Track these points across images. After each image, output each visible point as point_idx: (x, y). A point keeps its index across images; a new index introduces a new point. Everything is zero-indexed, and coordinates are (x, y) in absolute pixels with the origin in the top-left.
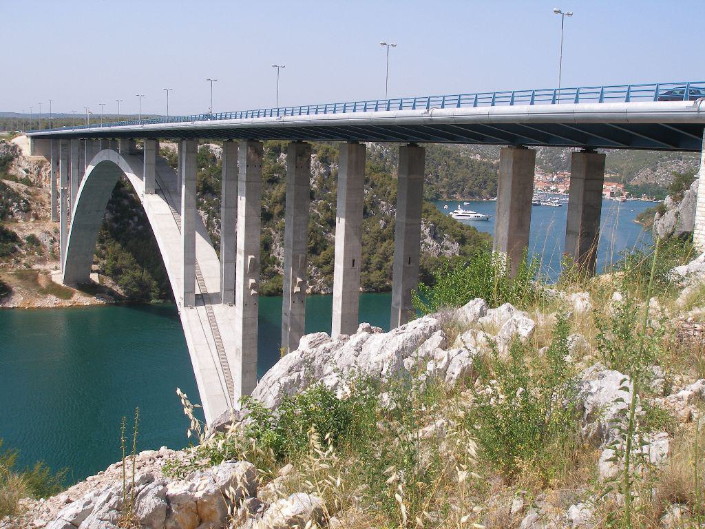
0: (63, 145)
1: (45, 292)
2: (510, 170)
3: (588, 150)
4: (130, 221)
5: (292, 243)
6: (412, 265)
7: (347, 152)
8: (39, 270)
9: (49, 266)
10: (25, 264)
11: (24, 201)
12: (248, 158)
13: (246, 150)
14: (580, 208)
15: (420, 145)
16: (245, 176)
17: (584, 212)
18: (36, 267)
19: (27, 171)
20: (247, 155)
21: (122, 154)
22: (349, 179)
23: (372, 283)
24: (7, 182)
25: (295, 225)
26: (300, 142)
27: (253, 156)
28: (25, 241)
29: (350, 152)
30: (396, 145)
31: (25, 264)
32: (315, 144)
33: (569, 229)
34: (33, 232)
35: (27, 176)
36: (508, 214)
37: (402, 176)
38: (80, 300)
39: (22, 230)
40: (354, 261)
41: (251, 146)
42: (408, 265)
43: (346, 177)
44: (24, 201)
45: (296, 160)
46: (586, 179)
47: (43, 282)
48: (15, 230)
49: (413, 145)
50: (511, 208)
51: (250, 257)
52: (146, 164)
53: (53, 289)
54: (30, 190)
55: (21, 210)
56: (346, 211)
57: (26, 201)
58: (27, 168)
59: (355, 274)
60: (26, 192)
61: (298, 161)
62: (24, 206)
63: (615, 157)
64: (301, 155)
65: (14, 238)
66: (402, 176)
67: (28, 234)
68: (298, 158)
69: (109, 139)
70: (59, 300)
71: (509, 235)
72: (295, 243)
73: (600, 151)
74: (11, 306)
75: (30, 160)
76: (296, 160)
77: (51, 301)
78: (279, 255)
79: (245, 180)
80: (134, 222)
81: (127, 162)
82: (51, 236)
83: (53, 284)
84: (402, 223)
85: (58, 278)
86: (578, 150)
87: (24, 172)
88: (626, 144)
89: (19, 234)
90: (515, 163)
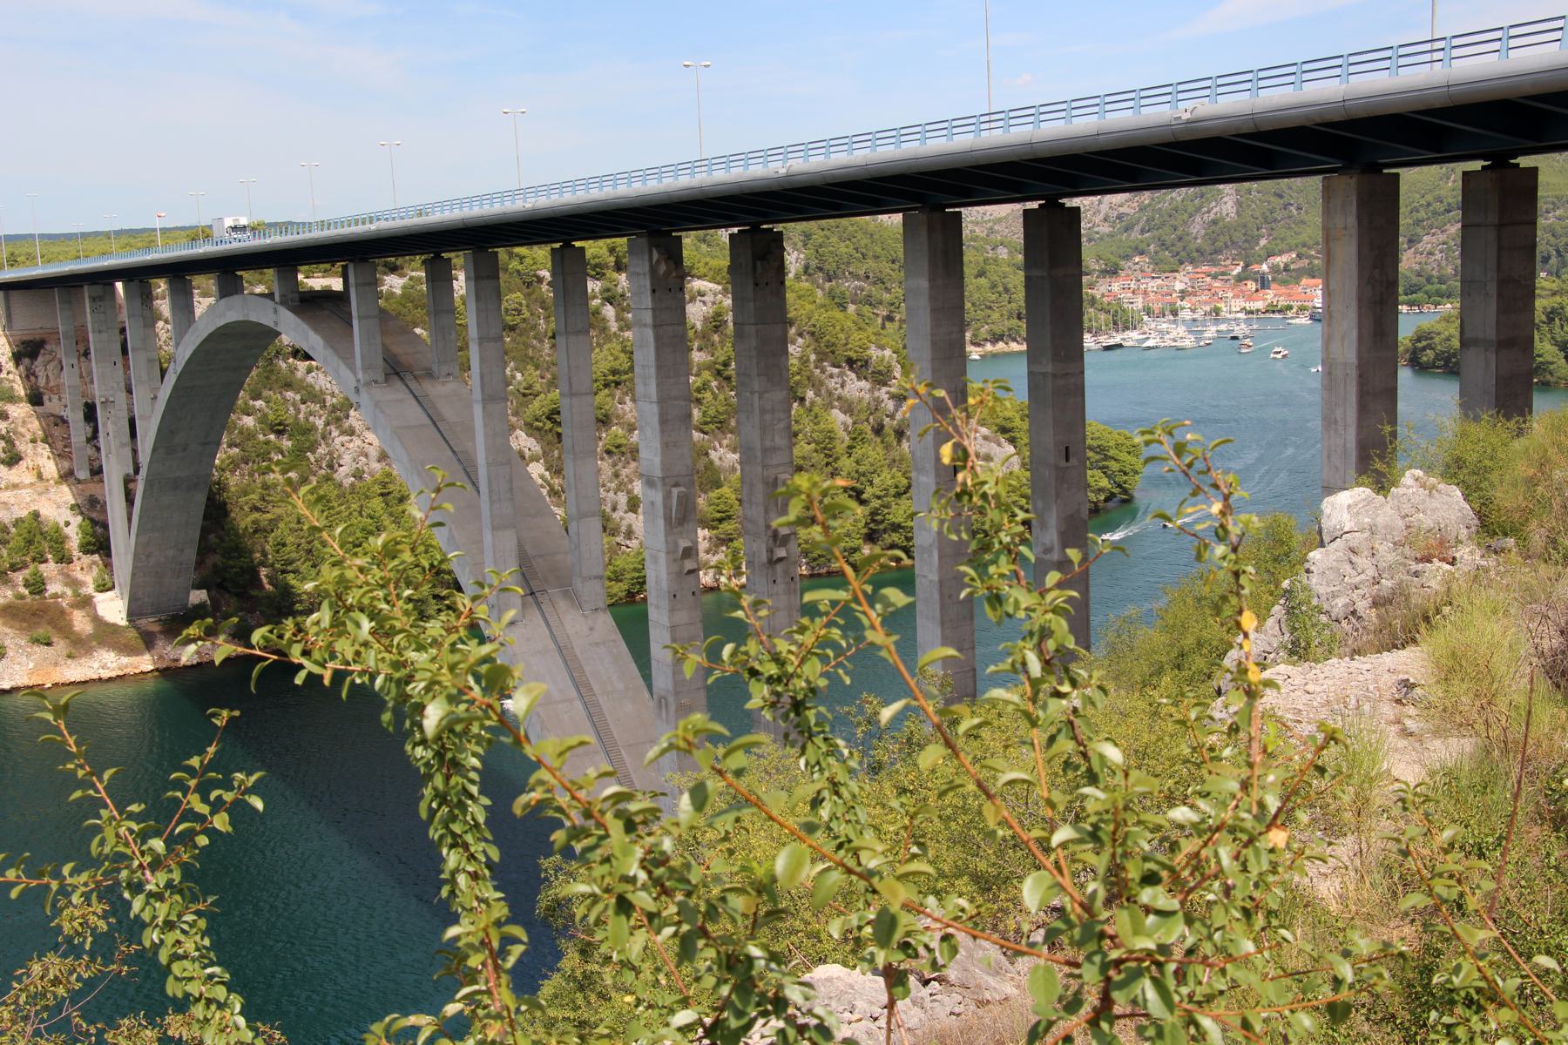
0: (93, 299)
1: (80, 646)
2: (1352, 221)
5: (759, 454)
6: (1073, 461)
7: (924, 232)
13: (647, 256)
14: (1492, 288)
16: (649, 313)
17: (1500, 295)
20: (651, 267)
21: (283, 303)
22: (931, 288)
26: (755, 228)
29: (931, 229)
30: (1018, 208)
32: (793, 231)
33: (1468, 335)
36: (1352, 315)
41: (657, 247)
42: (1063, 463)
45: (754, 268)
46: (1500, 226)
49: (1052, 205)
50: (1360, 300)
51: (675, 491)
52: (360, 318)
53: (106, 635)
61: (759, 270)
64: (763, 258)
66: (1036, 273)
68: (759, 263)
70: (125, 660)
71: (1360, 358)
76: (754, 268)
77: (106, 663)
78: (614, 509)
81: (302, 319)
84: (1044, 375)
85: (113, 608)
86: (1477, 165)
90: (1361, 204)
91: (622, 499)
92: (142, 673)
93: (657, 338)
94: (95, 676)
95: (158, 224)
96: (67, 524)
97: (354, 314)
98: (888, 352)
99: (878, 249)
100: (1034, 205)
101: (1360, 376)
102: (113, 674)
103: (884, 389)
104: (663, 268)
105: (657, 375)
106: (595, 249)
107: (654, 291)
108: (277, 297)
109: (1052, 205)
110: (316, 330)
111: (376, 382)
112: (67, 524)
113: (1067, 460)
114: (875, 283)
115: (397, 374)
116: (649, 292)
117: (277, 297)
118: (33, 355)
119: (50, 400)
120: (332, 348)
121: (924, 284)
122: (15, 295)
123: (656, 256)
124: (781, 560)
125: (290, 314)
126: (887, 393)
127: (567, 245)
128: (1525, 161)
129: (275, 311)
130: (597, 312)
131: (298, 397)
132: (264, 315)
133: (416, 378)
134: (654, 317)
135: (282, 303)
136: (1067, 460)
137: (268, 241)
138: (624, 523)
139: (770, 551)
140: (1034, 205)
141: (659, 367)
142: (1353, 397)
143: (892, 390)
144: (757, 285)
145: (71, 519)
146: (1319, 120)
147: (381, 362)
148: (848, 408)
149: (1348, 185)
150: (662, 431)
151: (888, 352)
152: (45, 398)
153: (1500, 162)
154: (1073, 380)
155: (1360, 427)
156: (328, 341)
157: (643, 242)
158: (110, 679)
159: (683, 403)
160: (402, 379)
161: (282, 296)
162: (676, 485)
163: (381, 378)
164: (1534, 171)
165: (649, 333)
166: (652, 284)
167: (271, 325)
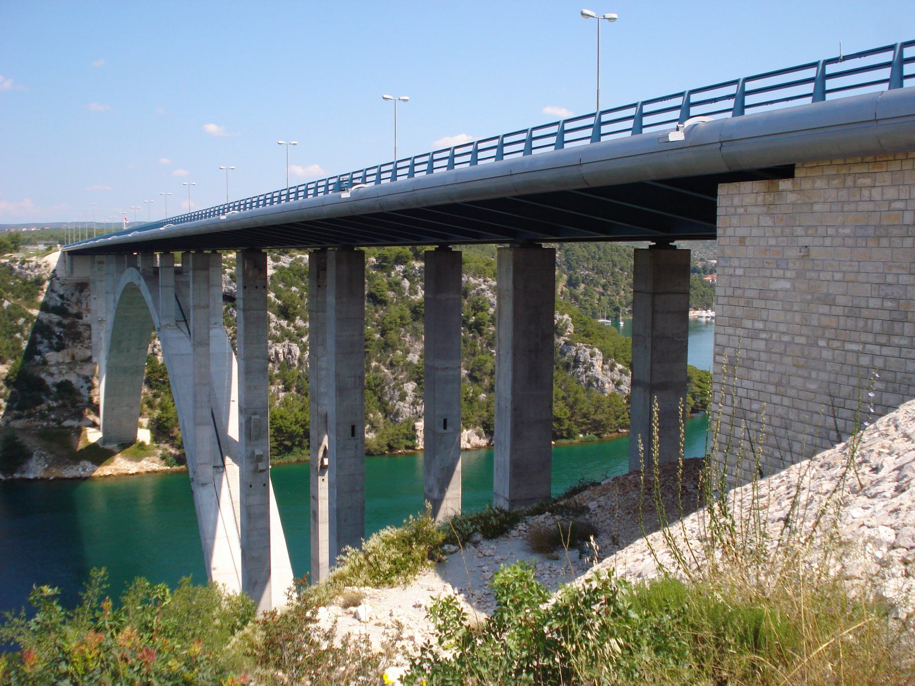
3: (663, 244)
6: (450, 429)
8: (71, 427)
10: (54, 420)
14: (649, 340)
15: (456, 248)
18: (68, 423)
19: (62, 297)
27: (251, 272)
28: (54, 389)
31: (54, 420)
34: (66, 377)
35: (62, 304)
37: (429, 296)
39: (52, 375)
40: (353, 428)
42: (441, 430)
43: (334, 301)
48: (43, 376)
49: (444, 249)
50: (515, 348)
54: (66, 322)
56: (337, 354)
57: (59, 337)
58: (61, 293)
59: (356, 447)
60: (59, 324)
62: (57, 343)
65: (41, 385)
67: (59, 379)
74: (31, 476)
75: (66, 283)
78: (391, 399)
79: (241, 307)
87: (58, 298)
89: (49, 381)
90: (516, 272)
91: (397, 393)
93: (245, 318)
94: (79, 476)
96: (82, 387)
98: (566, 316)
99: (602, 255)
103: (562, 338)
107: (245, 287)
109: (444, 249)
111: (170, 326)
112: (82, 387)
113: (445, 428)
114: (597, 273)
115: (185, 321)
118: (81, 291)
119: (86, 316)
122: (77, 259)
126: (564, 340)
128: (681, 244)
130: (398, 284)
134: (244, 304)
135: (142, 274)
136: (445, 428)
138: (397, 407)
143: (566, 338)
145: (84, 385)
146: (425, 205)
150: (246, 379)
151: (566, 316)
152: (84, 315)
154: (451, 373)
155: (513, 450)
159: (262, 361)
161: (143, 270)
162: (255, 414)
163: (173, 323)
164: (687, 252)
166: (244, 283)
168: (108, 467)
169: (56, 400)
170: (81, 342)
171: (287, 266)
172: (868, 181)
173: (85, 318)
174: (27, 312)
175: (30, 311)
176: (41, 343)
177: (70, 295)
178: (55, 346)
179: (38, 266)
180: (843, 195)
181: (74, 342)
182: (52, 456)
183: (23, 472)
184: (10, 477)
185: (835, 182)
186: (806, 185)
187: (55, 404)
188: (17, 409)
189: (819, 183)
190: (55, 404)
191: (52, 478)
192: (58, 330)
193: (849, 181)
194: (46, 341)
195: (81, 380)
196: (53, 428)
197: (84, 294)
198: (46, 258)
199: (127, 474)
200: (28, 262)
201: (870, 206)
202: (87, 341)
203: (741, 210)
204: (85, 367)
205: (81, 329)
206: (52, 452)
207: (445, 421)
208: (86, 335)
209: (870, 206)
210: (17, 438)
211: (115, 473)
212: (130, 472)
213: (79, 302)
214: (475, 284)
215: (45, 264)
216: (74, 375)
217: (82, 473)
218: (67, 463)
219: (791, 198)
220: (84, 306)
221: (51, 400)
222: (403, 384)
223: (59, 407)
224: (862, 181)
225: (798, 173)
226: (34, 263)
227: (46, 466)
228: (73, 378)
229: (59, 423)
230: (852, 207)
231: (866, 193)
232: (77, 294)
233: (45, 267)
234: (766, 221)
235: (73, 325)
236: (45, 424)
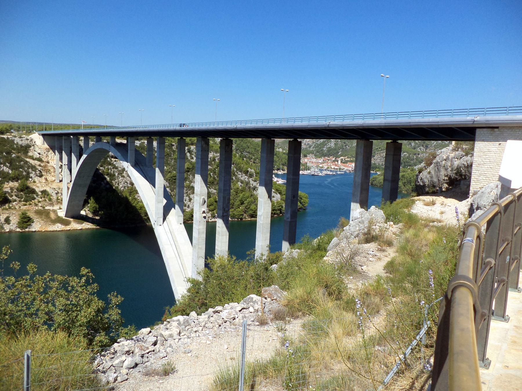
0: (65, 140)
1: (54, 222)
2: (362, 150)
4: (102, 183)
5: (223, 190)
6: (295, 199)
9: (56, 207)
10: (41, 206)
11: (39, 171)
12: (202, 146)
14: (391, 168)
15: (299, 140)
18: (47, 208)
19: (39, 154)
20: (202, 145)
21: (112, 145)
23: (236, 215)
24: (28, 160)
25: (225, 181)
28: (40, 193)
30: (288, 140)
31: (41, 206)
34: (45, 188)
35: (40, 157)
38: (75, 226)
39: (38, 187)
42: (293, 199)
44: (39, 171)
45: (225, 148)
46: (394, 155)
47: (52, 216)
48: (34, 187)
49: (295, 140)
50: (363, 168)
52: (130, 150)
53: (59, 220)
54: (42, 164)
55: (37, 175)
58: (39, 152)
60: (40, 165)
61: (227, 148)
62: (39, 174)
63: (406, 144)
65: (33, 191)
67: (42, 189)
68: (227, 147)
69: (99, 136)
70: (63, 227)
72: (224, 190)
73: (400, 142)
74: (34, 230)
75: (41, 147)
76: (225, 148)
77: (59, 227)
80: (104, 183)
81: (116, 149)
82: (56, 190)
83: (59, 217)
85: (62, 214)
86: (390, 141)
87: (38, 154)
88: (426, 138)
89: (37, 190)
90: (365, 147)
92: (67, 230)
93: (201, 162)
94: (56, 230)
95: (83, 123)
97: (129, 149)
100: (292, 140)
101: (361, 185)
102: (60, 230)
103: (251, 179)
104: (204, 146)
105: (201, 171)
106: (188, 140)
107: (202, 151)
108: (110, 143)
110: (119, 152)
116: (201, 151)
117: (110, 143)
120: (123, 156)
121: (265, 155)
122: (46, 137)
123: (203, 143)
124: (225, 216)
125: (113, 148)
127: (182, 138)
129: (110, 147)
131: (112, 167)
132: (107, 147)
133: (142, 166)
137: (110, 130)
139: (223, 213)
140: (292, 140)
141: (201, 168)
142: (359, 190)
144: (226, 152)
146: (357, 128)
147: (134, 161)
148: (242, 182)
149: (362, 142)
151: (253, 170)
153: (395, 141)
155: (360, 197)
156: (121, 154)
157: (200, 139)
158: (59, 231)
160: (139, 166)
161: (111, 143)
164: (401, 144)
165: (200, 160)
167: (108, 150)
168: (68, 226)
169: (41, 198)
170: (50, 173)
171: (138, 145)
172: (518, 130)
173: (50, 163)
174: (25, 160)
175: (25, 159)
176: (32, 173)
177: (43, 153)
178: (38, 175)
179: (27, 139)
180: (512, 133)
181: (47, 173)
182: (42, 222)
183: (30, 228)
184: (23, 230)
185: (510, 130)
186: (501, 130)
187: (40, 200)
188: (24, 201)
189: (505, 130)
190: (40, 200)
191: (43, 231)
192: (39, 168)
193: (514, 130)
194: (34, 172)
195: (51, 189)
196: (41, 210)
197: (49, 153)
198: (30, 136)
199: (77, 229)
200: (23, 137)
201: (518, 135)
202: (53, 174)
203: (483, 134)
204: (53, 184)
205: (49, 168)
206: (43, 220)
207: (294, 196)
208: (52, 170)
209: (518, 135)
210: (27, 213)
211: (72, 229)
212: (78, 229)
213: (47, 156)
214: (216, 156)
215: (30, 139)
216: (48, 187)
217: (57, 228)
218: (50, 224)
219: (498, 132)
220: (50, 158)
221: (39, 198)
222: (190, 195)
223: (42, 201)
224: (516, 130)
225: (499, 128)
226: (25, 138)
227: (40, 226)
228: (48, 189)
229: (44, 208)
230: (514, 135)
231: (518, 132)
232: (46, 153)
233: (31, 140)
234: (492, 137)
235: (45, 166)
236: (37, 208)
